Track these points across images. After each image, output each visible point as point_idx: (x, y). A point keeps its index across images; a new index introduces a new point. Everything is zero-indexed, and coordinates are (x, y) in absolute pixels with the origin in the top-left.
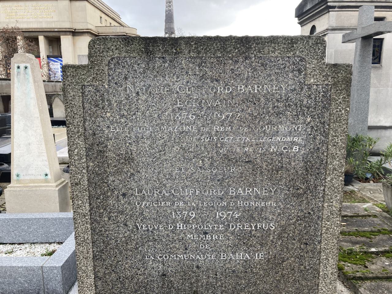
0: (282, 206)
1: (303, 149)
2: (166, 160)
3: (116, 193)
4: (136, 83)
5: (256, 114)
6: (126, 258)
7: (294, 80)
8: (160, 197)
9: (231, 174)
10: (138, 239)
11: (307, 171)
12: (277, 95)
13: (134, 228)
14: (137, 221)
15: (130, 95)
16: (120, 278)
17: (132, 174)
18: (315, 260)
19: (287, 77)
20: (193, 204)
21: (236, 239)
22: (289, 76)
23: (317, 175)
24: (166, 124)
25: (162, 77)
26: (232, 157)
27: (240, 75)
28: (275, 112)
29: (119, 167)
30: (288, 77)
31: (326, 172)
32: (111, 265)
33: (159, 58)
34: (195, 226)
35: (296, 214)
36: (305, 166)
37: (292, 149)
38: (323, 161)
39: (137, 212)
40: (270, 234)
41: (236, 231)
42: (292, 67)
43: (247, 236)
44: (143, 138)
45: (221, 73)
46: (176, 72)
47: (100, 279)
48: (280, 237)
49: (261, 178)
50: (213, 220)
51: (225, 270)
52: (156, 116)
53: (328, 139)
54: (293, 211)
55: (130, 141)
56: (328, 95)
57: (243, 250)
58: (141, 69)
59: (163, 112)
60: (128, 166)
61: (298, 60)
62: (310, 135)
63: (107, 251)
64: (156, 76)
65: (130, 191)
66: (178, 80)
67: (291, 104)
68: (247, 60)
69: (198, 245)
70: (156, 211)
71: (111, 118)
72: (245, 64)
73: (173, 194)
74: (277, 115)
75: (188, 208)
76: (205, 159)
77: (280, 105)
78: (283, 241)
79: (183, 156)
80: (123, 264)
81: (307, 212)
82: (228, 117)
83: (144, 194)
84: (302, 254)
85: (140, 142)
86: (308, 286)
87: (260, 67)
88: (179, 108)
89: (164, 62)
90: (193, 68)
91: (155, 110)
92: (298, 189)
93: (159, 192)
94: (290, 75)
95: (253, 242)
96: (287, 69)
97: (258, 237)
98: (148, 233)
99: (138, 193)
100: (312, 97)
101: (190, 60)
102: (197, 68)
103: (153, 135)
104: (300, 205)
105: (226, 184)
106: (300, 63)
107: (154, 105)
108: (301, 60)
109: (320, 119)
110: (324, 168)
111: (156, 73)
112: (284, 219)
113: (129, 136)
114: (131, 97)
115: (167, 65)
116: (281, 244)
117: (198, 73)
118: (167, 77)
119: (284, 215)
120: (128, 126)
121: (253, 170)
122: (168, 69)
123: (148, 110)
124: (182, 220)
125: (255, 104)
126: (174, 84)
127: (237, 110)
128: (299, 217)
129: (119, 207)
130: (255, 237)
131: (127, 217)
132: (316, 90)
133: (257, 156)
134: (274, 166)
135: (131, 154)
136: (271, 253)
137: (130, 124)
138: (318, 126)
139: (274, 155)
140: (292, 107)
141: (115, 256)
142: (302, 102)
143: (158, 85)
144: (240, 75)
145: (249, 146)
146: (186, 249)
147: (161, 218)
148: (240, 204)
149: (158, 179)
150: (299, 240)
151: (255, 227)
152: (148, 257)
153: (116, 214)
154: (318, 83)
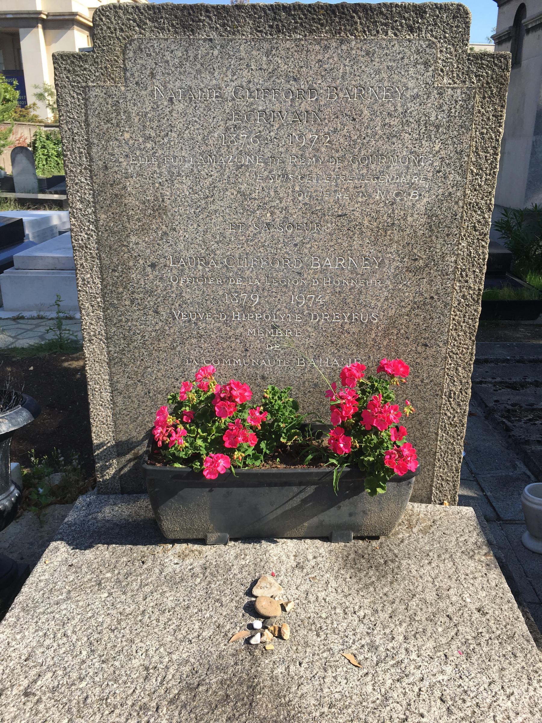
0: (391, 287)
1: (427, 195)
2: (216, 211)
3: (141, 263)
4: (169, 82)
5: (356, 137)
6: (159, 362)
7: (417, 79)
8: (207, 269)
9: (315, 235)
10: (175, 333)
11: (432, 231)
12: (390, 104)
13: (169, 317)
14: (173, 307)
15: (159, 103)
16: (149, 393)
17: (165, 233)
18: (438, 370)
19: (406, 73)
20: (257, 282)
21: (320, 335)
22: (410, 73)
23: (446, 238)
24: (215, 153)
25: (209, 72)
26: (317, 208)
27: (331, 70)
28: (384, 134)
29: (144, 221)
30: (408, 74)
31: (460, 232)
32: (136, 373)
33: (205, 40)
34: (259, 316)
35: (411, 298)
36: (428, 223)
37: (410, 195)
38: (456, 216)
39: (173, 292)
40: (372, 330)
41: (321, 323)
42: (415, 57)
43: (336, 331)
44: (179, 175)
45: (302, 67)
46: (230, 65)
47: (121, 393)
48: (386, 334)
49: (360, 242)
50: (286, 307)
51: (304, 383)
52: (200, 138)
53: (466, 178)
54: (407, 294)
55: (160, 181)
56: (470, 107)
57: (330, 353)
58: (176, 60)
59: (210, 132)
60: (158, 221)
61: (424, 46)
62: (439, 172)
63: (129, 351)
64: (199, 72)
65: (162, 260)
66: (235, 77)
67: (411, 120)
68: (343, 46)
69: (264, 345)
70: (201, 292)
71: (131, 142)
72: (339, 52)
73: (226, 266)
74: (388, 138)
75: (249, 289)
76: (276, 211)
77: (394, 122)
78: (390, 339)
79: (241, 205)
80: (153, 372)
81: (428, 297)
82: (312, 142)
83: (183, 265)
84: (418, 361)
85: (176, 181)
86: (425, 408)
87: (363, 56)
88: (236, 126)
89: (212, 48)
90: (257, 58)
91: (198, 129)
92: (416, 259)
93: (205, 263)
94: (412, 70)
95: (345, 342)
96: (406, 61)
97: (354, 333)
98: (190, 325)
99: (174, 264)
100: (444, 108)
101: (253, 43)
102: (265, 58)
103: (195, 170)
104: (419, 285)
105: (306, 251)
106: (428, 50)
107: (197, 120)
108: (429, 45)
109: (456, 146)
110: (457, 227)
111: (199, 66)
112: (393, 306)
113: (158, 172)
114: (161, 107)
115: (216, 52)
116: (387, 345)
117: (265, 67)
118: (216, 73)
119: (393, 300)
120: (157, 155)
121: (348, 229)
122: (219, 59)
123: (187, 128)
124: (241, 306)
125: (354, 120)
126: (227, 86)
127: (326, 130)
128: (415, 303)
129: (146, 284)
130: (349, 333)
131: (159, 300)
132: (451, 98)
133: (356, 205)
134: (380, 223)
135: (163, 201)
136: (372, 357)
137: (160, 152)
138: (451, 158)
139: (381, 205)
140: (413, 125)
141: (142, 360)
142: (429, 117)
143: (202, 86)
144: (331, 70)
145: (343, 190)
146: (246, 350)
147: (209, 302)
148: (328, 283)
149: (204, 242)
150: (415, 340)
151: (349, 318)
152: (189, 362)
153: (141, 295)
154: (456, 85)
